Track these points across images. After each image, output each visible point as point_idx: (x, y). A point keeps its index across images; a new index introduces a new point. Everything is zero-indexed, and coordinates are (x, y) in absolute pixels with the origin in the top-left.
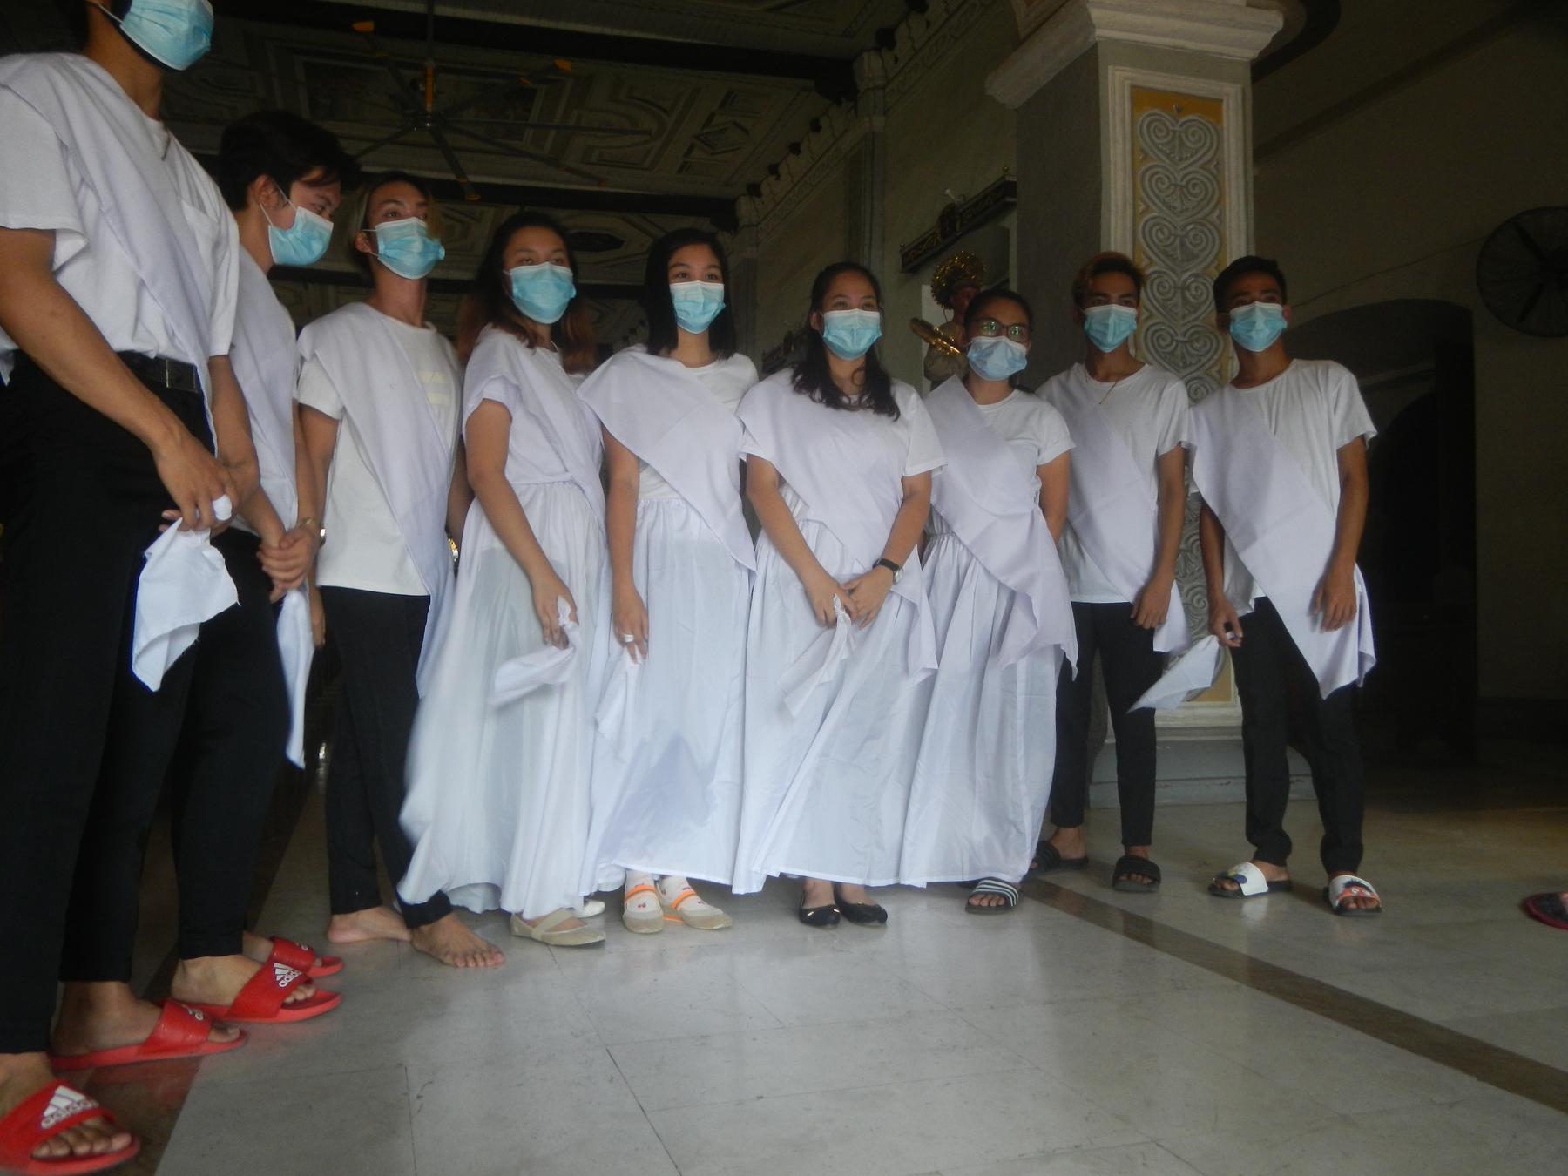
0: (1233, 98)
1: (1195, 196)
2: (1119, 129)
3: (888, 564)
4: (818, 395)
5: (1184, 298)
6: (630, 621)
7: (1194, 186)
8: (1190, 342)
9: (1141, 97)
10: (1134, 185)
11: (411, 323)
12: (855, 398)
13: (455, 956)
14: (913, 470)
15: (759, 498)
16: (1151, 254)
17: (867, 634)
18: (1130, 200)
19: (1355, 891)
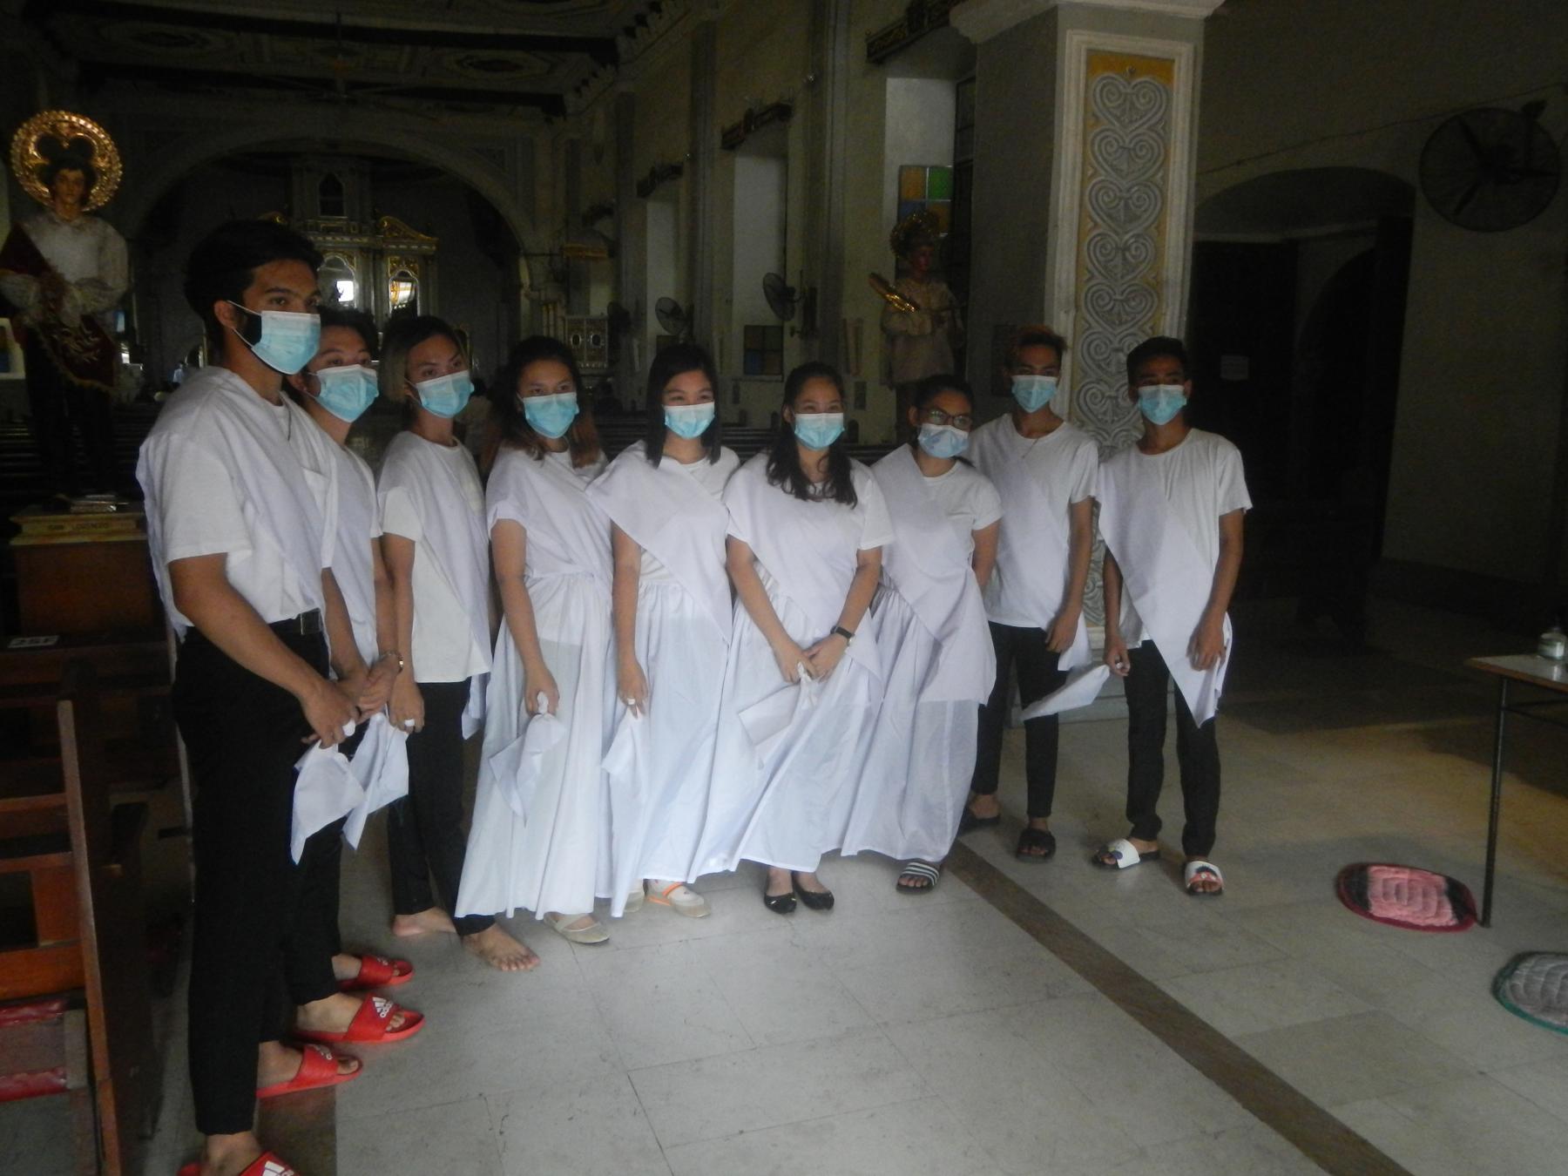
0: (1184, 56)
2: (1073, 95)
3: (842, 632)
4: (788, 486)
6: (631, 684)
8: (1127, 300)
9: (1097, 60)
10: (1084, 153)
11: (447, 444)
12: (819, 486)
13: (501, 962)
14: (867, 545)
15: (741, 575)
17: (823, 689)
18: (1079, 165)
19: (1204, 876)
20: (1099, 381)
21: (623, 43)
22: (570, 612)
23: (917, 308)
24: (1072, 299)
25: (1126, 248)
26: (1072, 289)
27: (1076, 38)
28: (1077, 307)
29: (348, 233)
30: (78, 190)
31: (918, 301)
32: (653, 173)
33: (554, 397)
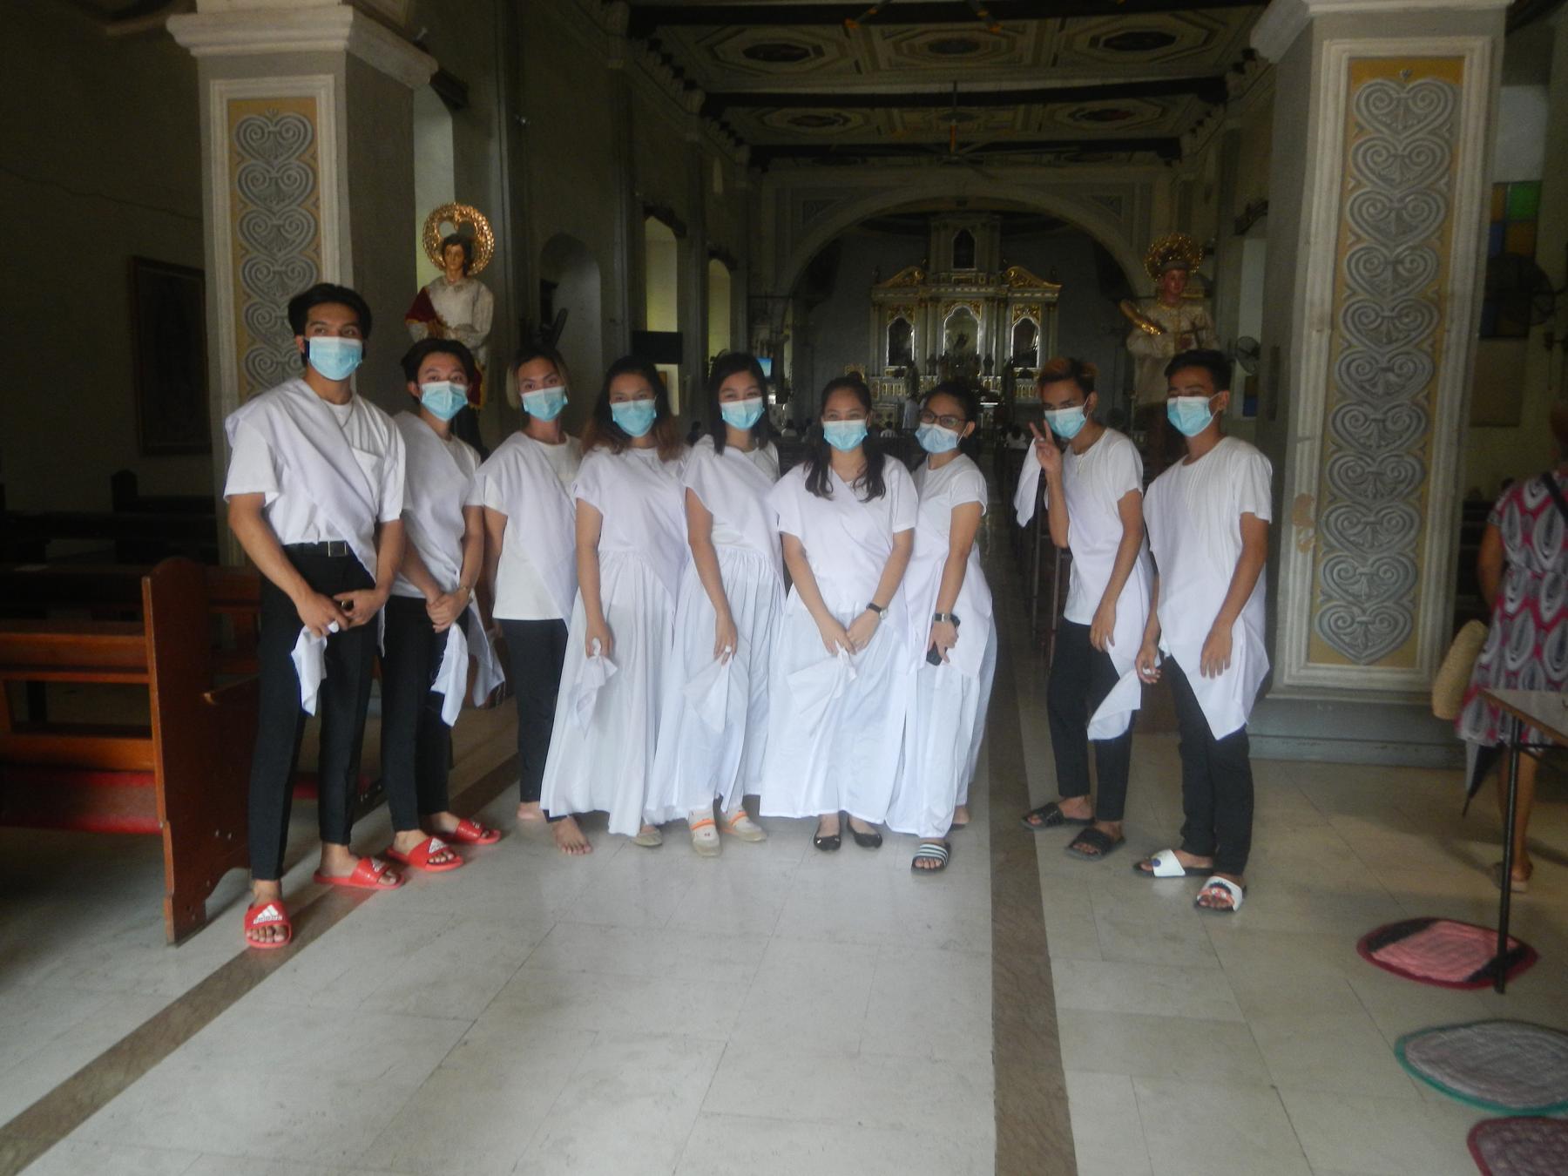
1: (1416, 164)
2: (1331, 106)
5: (1395, 271)
7: (1418, 155)
8: (1399, 317)
9: (1359, 68)
16: (1357, 229)
18: (1338, 179)
19: (1215, 891)
20: (1361, 402)
21: (1232, 79)
22: (627, 574)
23: (1163, 330)
24: (1327, 319)
25: (1399, 261)
26: (1328, 307)
27: (1333, 48)
28: (1333, 326)
29: (976, 284)
30: (459, 260)
31: (1165, 324)
32: (1248, 209)
33: (631, 403)
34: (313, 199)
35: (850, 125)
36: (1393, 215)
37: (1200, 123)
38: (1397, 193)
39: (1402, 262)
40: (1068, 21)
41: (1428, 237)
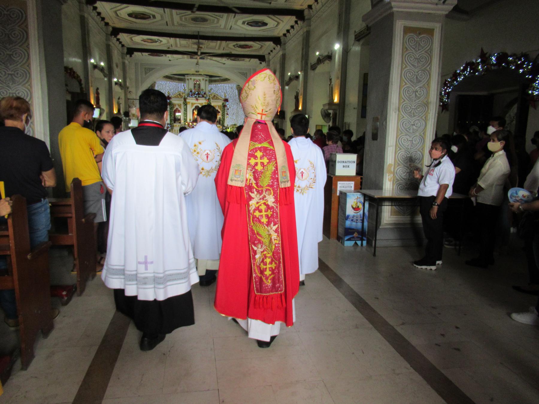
5: (416, 95)
8: (416, 109)
9: (407, 30)
20: (406, 135)
25: (417, 91)
26: (397, 105)
27: (400, 23)
28: (399, 111)
34: (26, 44)
35: (162, 43)
36: (415, 77)
37: (272, 51)
38: (416, 70)
39: (417, 92)
40: (237, 15)
41: (424, 85)
